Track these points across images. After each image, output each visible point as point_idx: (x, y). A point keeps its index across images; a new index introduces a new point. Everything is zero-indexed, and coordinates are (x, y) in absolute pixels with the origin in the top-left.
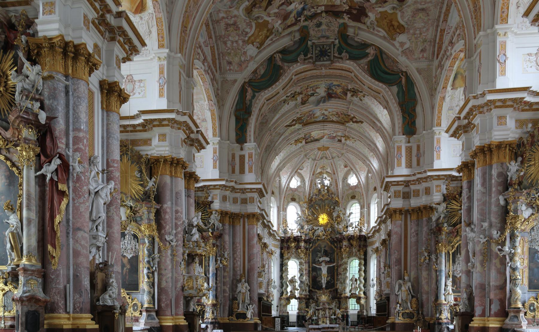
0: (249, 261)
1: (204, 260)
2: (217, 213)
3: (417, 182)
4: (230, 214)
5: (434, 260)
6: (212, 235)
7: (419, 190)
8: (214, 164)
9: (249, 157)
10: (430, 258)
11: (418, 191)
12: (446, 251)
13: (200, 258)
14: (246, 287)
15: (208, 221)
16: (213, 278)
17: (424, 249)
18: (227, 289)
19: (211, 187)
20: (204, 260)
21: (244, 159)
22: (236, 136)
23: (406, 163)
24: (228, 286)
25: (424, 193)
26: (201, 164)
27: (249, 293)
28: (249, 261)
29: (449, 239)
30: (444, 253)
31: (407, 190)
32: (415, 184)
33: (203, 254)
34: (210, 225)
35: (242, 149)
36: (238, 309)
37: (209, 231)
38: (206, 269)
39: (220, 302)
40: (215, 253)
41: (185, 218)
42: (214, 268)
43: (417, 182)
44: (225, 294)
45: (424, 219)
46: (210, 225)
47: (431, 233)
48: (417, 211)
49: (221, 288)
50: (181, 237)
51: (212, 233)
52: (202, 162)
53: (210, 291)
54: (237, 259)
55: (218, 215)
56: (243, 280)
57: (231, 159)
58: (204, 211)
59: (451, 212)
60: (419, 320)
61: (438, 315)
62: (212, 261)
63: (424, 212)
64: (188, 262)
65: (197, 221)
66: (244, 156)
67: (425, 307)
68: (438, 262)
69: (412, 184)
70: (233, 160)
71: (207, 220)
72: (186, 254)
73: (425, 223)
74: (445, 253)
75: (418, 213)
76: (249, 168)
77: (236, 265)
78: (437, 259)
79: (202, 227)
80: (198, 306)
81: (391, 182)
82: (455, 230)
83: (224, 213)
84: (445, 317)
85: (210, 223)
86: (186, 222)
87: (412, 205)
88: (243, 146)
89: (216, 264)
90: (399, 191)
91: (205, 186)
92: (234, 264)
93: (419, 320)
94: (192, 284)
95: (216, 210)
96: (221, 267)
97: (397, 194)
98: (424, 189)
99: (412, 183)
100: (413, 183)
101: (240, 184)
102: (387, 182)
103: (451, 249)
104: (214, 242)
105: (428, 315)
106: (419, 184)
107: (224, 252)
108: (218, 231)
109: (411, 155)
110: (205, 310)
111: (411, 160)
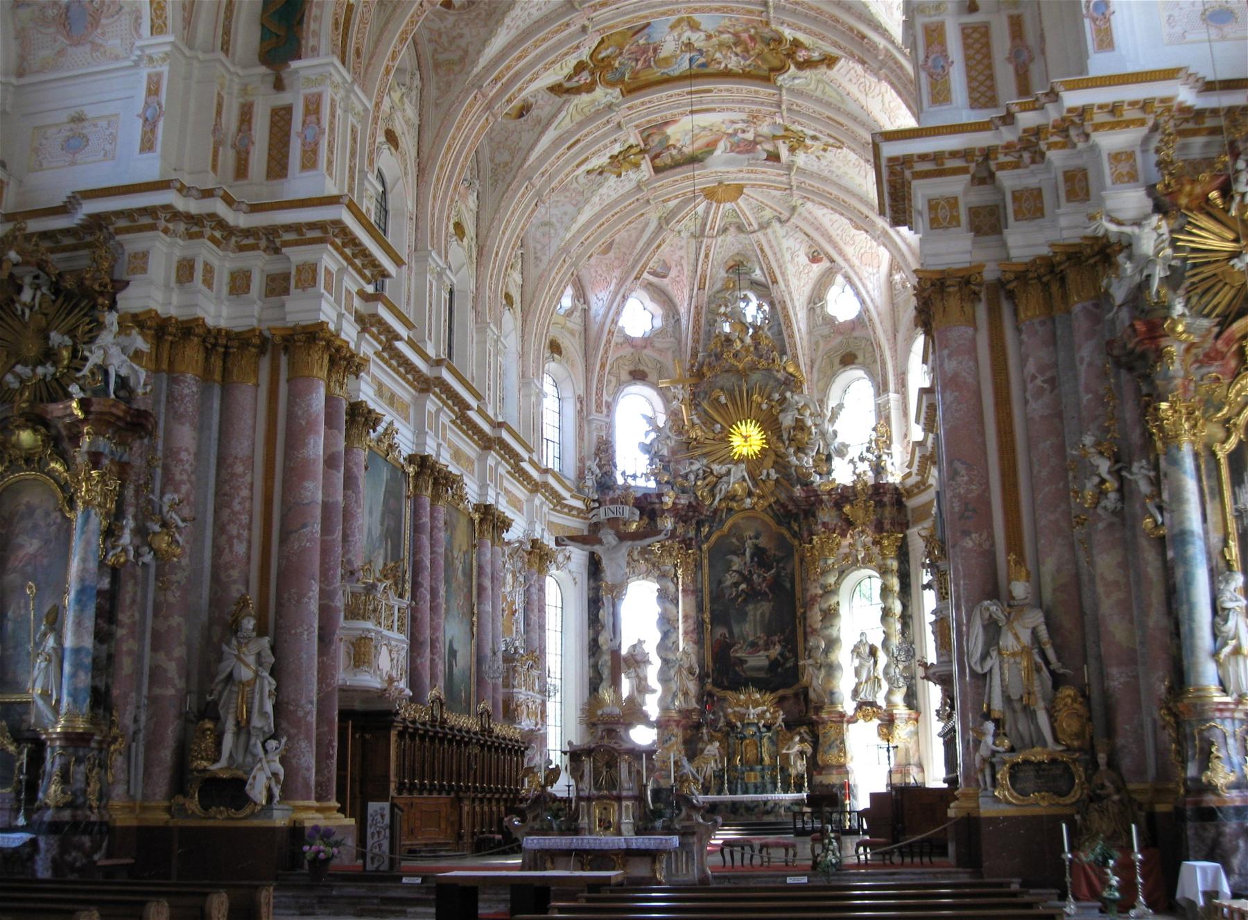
0: (283, 540)
3: (1026, 156)
5: (1144, 487)
7: (1040, 190)
8: (144, 134)
9: (307, 112)
10: (1121, 480)
11: (1038, 193)
12: (1199, 447)
14: (259, 654)
17: (1088, 440)
18: (172, 669)
19: (122, 223)
21: (289, 122)
22: (262, 39)
23: (971, 90)
24: (179, 652)
25: (1062, 194)
26: (108, 147)
27: (269, 683)
28: (284, 538)
29: (1203, 390)
30: (1186, 451)
31: (982, 196)
32: (1016, 165)
35: (279, 86)
36: (216, 760)
37: (69, 397)
43: (1026, 156)
44: (158, 691)
45: (1077, 308)
47: (1118, 363)
48: (1039, 278)
49: (139, 658)
51: (84, 404)
52: (113, 138)
54: (233, 529)
56: (249, 624)
57: (231, 120)
59: (1195, 266)
60: (1100, 798)
61: (1192, 771)
63: (1071, 276)
66: (288, 109)
67: (1124, 726)
68: (1165, 496)
69: (1002, 167)
70: (245, 127)
73: (1081, 324)
74: (1196, 455)
75: (1046, 286)
76: (304, 152)
77: (227, 557)
78: (1156, 483)
81: (906, 161)
82: (1228, 343)
84: (1232, 778)
87: (1014, 253)
88: (284, 75)
90: (953, 202)
91: (98, 222)
92: (218, 551)
93: (1100, 798)
97: (941, 213)
98: (1061, 179)
99: (1002, 158)
100: (1009, 159)
101: (255, 208)
102: (892, 160)
103: (1221, 434)
104: (104, 444)
105: (1140, 772)
106: (1033, 162)
109: (988, 56)
111: (991, 77)
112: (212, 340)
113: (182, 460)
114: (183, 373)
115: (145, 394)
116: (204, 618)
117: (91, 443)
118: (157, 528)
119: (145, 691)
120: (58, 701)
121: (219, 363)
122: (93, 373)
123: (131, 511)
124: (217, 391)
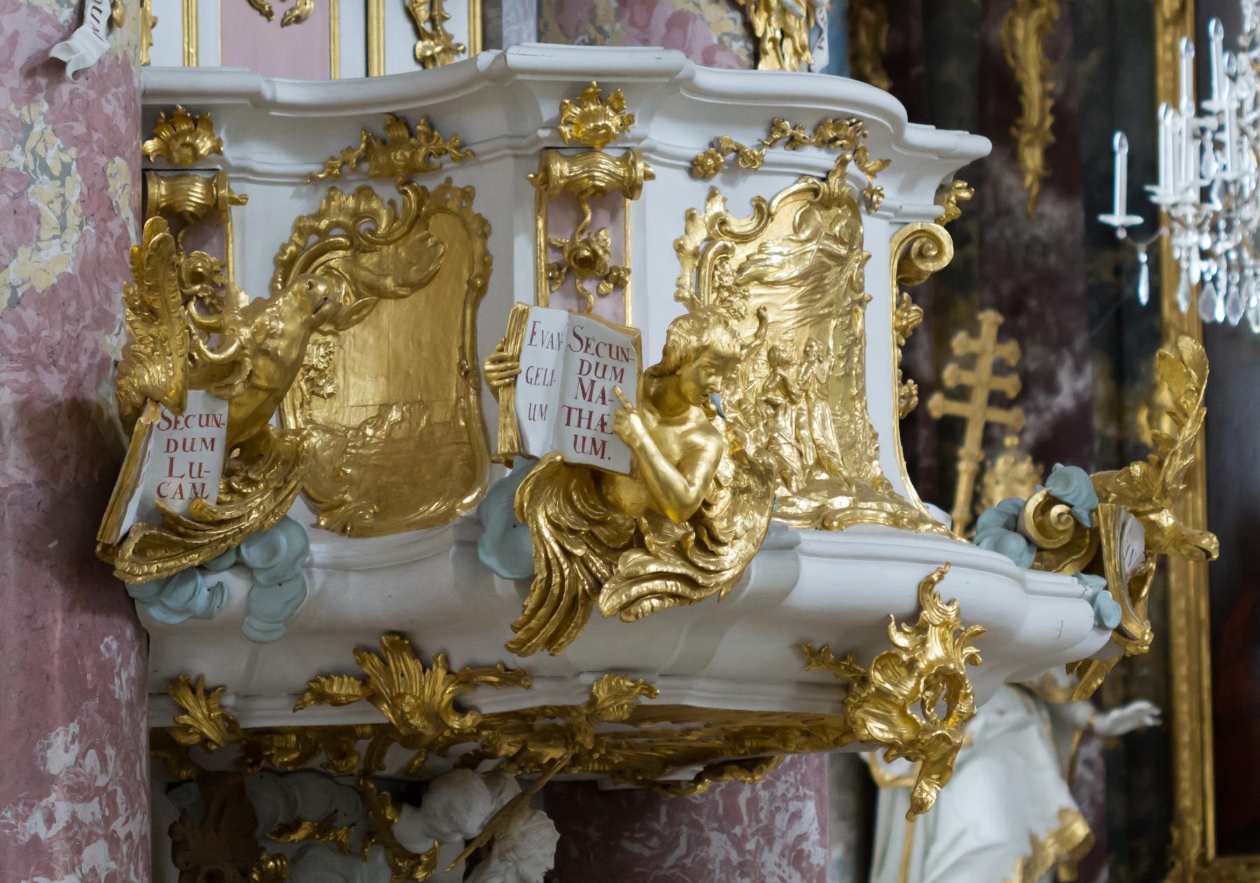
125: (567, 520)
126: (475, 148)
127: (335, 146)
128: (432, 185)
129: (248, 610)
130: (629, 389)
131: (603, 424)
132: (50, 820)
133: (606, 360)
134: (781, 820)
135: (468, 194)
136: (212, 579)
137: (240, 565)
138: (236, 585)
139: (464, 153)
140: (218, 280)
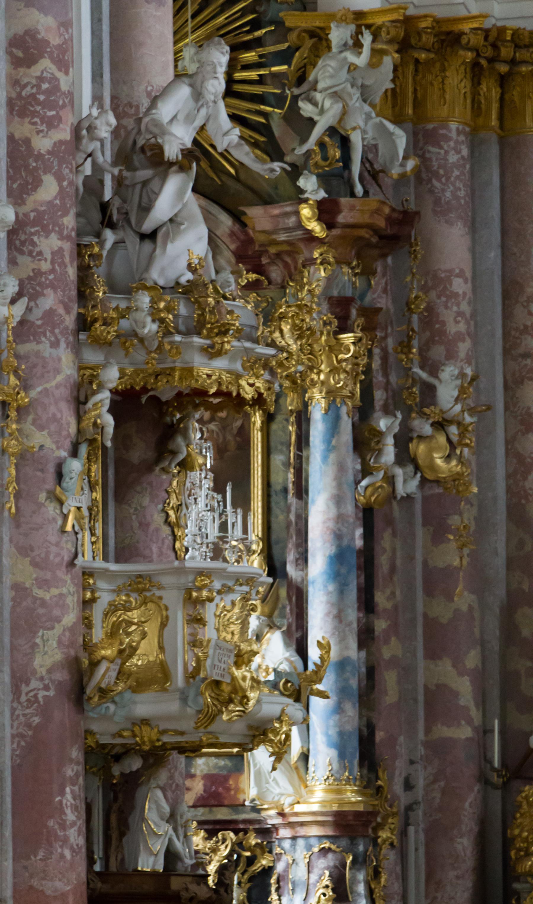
1: (257, 437)
2: (367, 39)
4: (477, 40)
6: (330, 225)
13: (224, 426)
15: (294, 109)
16: (341, 591)
20: (257, 437)
33: (249, 393)
34: (311, 143)
38: (279, 518)
39: (404, 799)
40: (353, 375)
41: (97, 98)
42: (349, 509)
46: (311, 143)
50: (58, 253)
53: (316, 702)
55: (376, 53)
58: (255, 25)
62: (330, 448)
64: (119, 463)
65: (189, 119)
71: (279, 101)
72: (105, 396)
79: (240, 166)
80: (211, 834)
83: (428, 39)
85: (311, 122)
86: (104, 132)
89: (366, 471)
94: (152, 639)
95: (359, 15)
96: (409, 498)
107: (434, 371)
108: (376, 196)
110: (268, 871)
112: (489, 52)
113: (456, 295)
114: (444, 123)
115: (403, 176)
116: (501, 591)
117: (329, 280)
118: (427, 430)
119: (421, 735)
120: (305, 757)
121: (495, 93)
122: (322, 145)
123: (379, 395)
124: (494, 150)
125: (213, 695)
126: (165, 586)
127: (120, 582)
128: (148, 594)
129: (114, 714)
130: (232, 660)
131: (224, 669)
132: (73, 770)
133: (225, 652)
134: (178, 764)
135: (160, 598)
136: (106, 705)
137: (113, 702)
138: (112, 707)
139: (160, 587)
140: (91, 619)
